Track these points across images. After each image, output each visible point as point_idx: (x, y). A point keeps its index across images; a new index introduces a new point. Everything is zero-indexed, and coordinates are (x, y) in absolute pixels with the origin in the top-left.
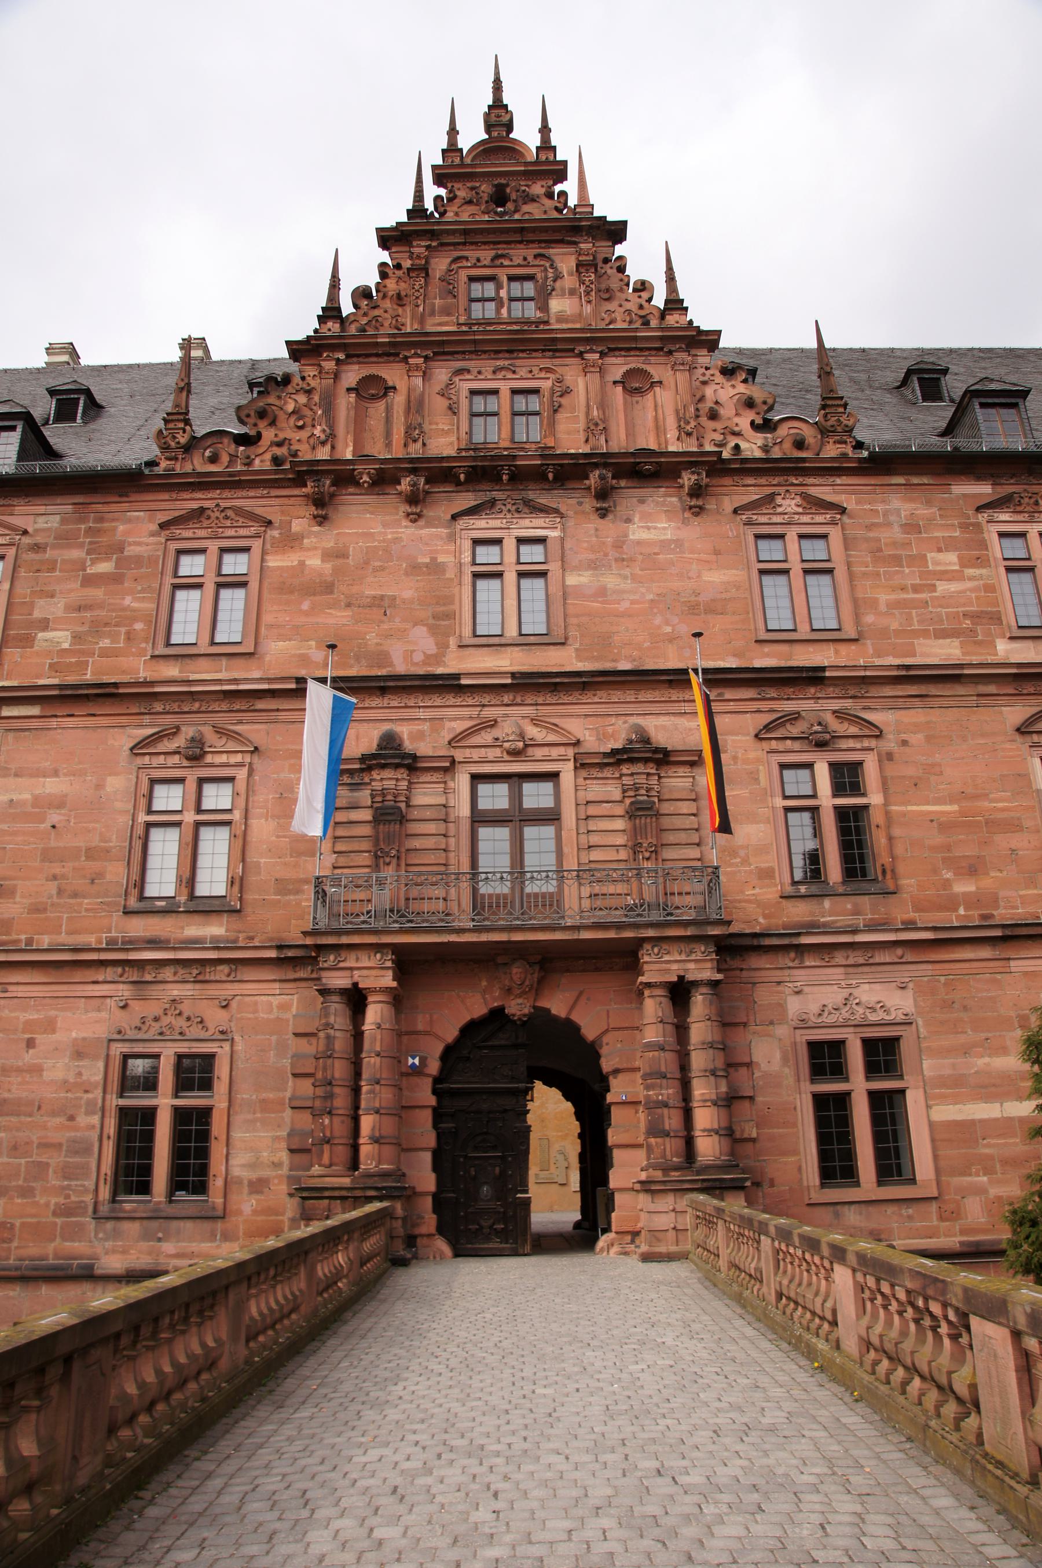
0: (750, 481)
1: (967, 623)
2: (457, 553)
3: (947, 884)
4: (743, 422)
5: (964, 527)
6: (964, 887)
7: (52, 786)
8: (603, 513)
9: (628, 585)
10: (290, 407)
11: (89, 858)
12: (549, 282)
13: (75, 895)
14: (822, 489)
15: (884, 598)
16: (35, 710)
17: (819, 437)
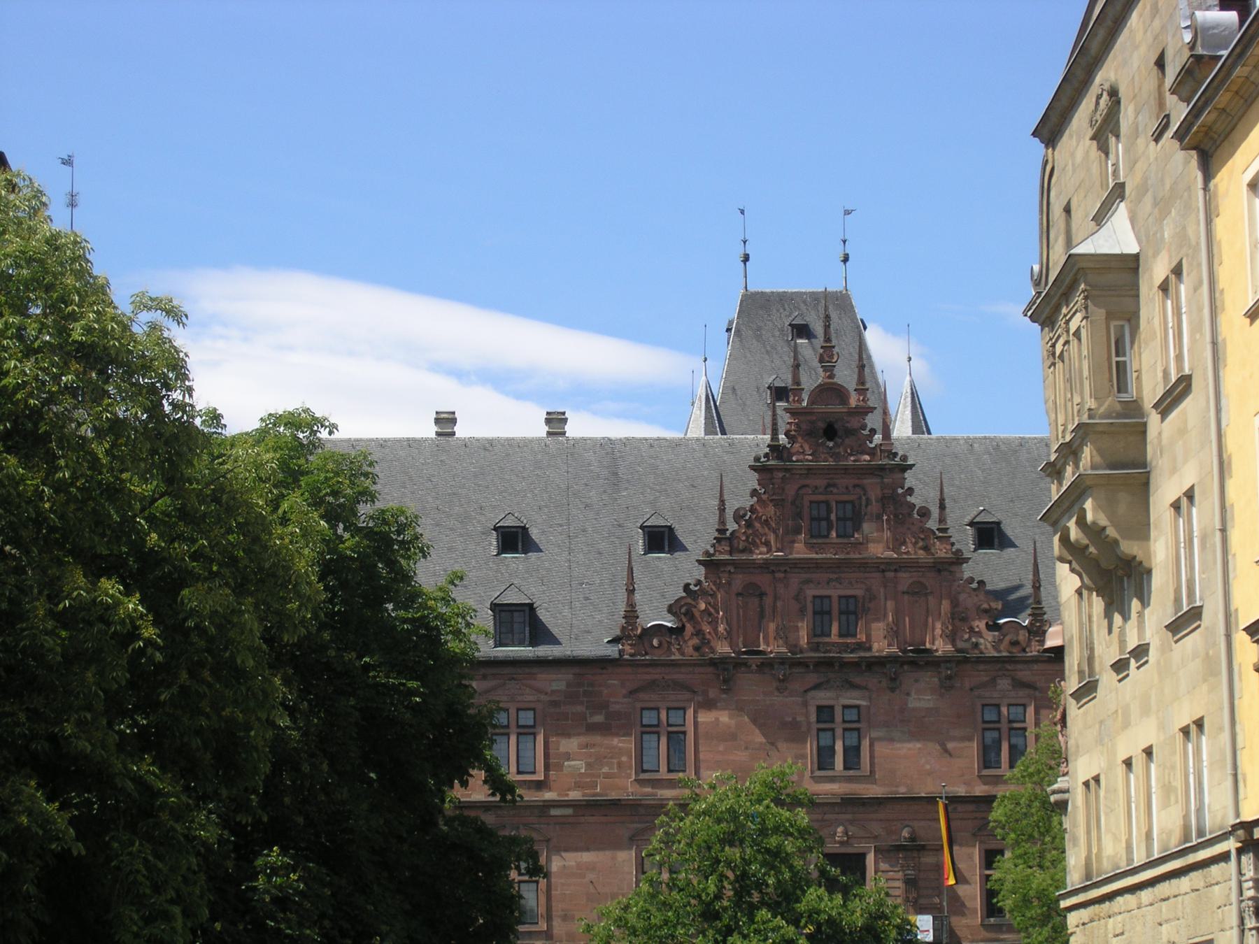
0: (982, 667)
2: (807, 715)
8: (893, 690)
10: (703, 606)
12: (863, 507)
14: (1025, 674)
16: (569, 811)
17: (1027, 635)
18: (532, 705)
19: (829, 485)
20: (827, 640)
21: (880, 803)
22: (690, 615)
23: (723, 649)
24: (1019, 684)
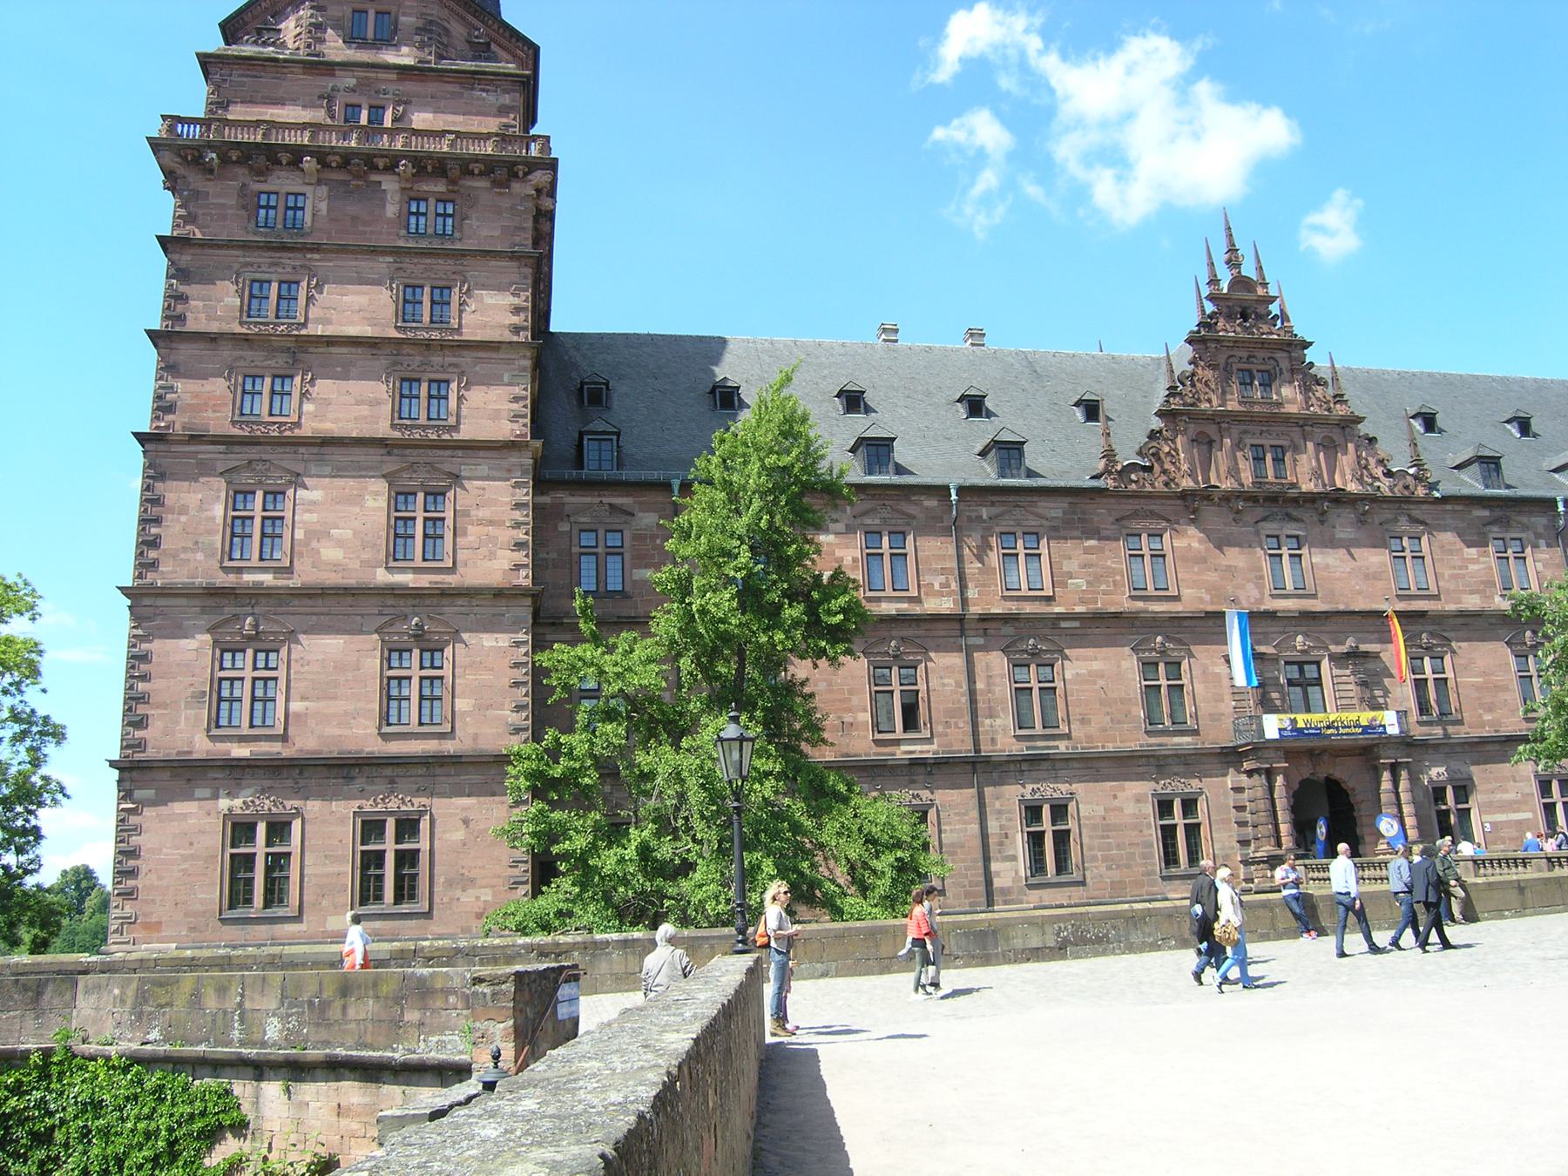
0: (1385, 506)
1: (1482, 587)
3: (1481, 715)
4: (1379, 472)
5: (1479, 534)
6: (1487, 717)
7: (1096, 666)
9: (1338, 563)
10: (1167, 449)
11: (1122, 703)
13: (1119, 722)
14: (1417, 513)
15: (1447, 573)
16: (1076, 624)
18: (1034, 530)
19: (1250, 357)
20: (1266, 480)
21: (1327, 618)
22: (1156, 455)
23: (1187, 483)
24: (1414, 521)
